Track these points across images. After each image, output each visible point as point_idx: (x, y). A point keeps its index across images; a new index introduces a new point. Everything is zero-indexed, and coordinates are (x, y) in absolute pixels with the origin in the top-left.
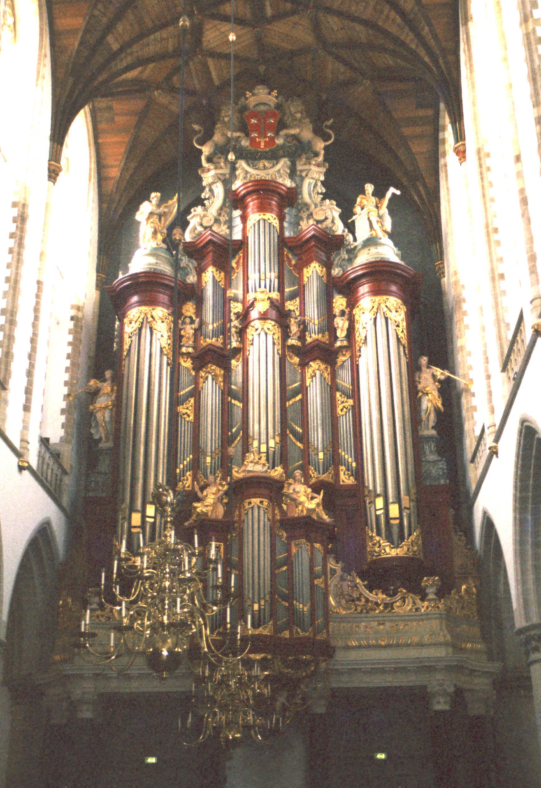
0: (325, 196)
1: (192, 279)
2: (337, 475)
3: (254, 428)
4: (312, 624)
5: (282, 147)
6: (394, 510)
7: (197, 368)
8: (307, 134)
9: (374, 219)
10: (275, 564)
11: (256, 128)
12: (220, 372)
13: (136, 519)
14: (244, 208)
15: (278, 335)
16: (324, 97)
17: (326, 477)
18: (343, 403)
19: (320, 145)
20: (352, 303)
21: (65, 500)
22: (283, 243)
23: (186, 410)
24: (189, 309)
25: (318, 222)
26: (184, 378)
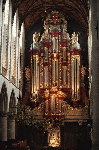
0: (67, 32)
1: (42, 48)
2: (67, 86)
3: (53, 78)
4: (61, 113)
5: (59, 22)
6: (76, 93)
7: (44, 66)
8: (63, 19)
9: (75, 39)
10: (56, 104)
11: (54, 18)
12: (47, 67)
13: (34, 94)
14: (52, 36)
15: (57, 61)
16: (67, 11)
17: (65, 87)
18: (69, 73)
19: (66, 22)
20: (71, 55)
21: (22, 89)
22: (59, 42)
23: (42, 74)
24: (42, 54)
25: (65, 38)
26: (41, 68)
